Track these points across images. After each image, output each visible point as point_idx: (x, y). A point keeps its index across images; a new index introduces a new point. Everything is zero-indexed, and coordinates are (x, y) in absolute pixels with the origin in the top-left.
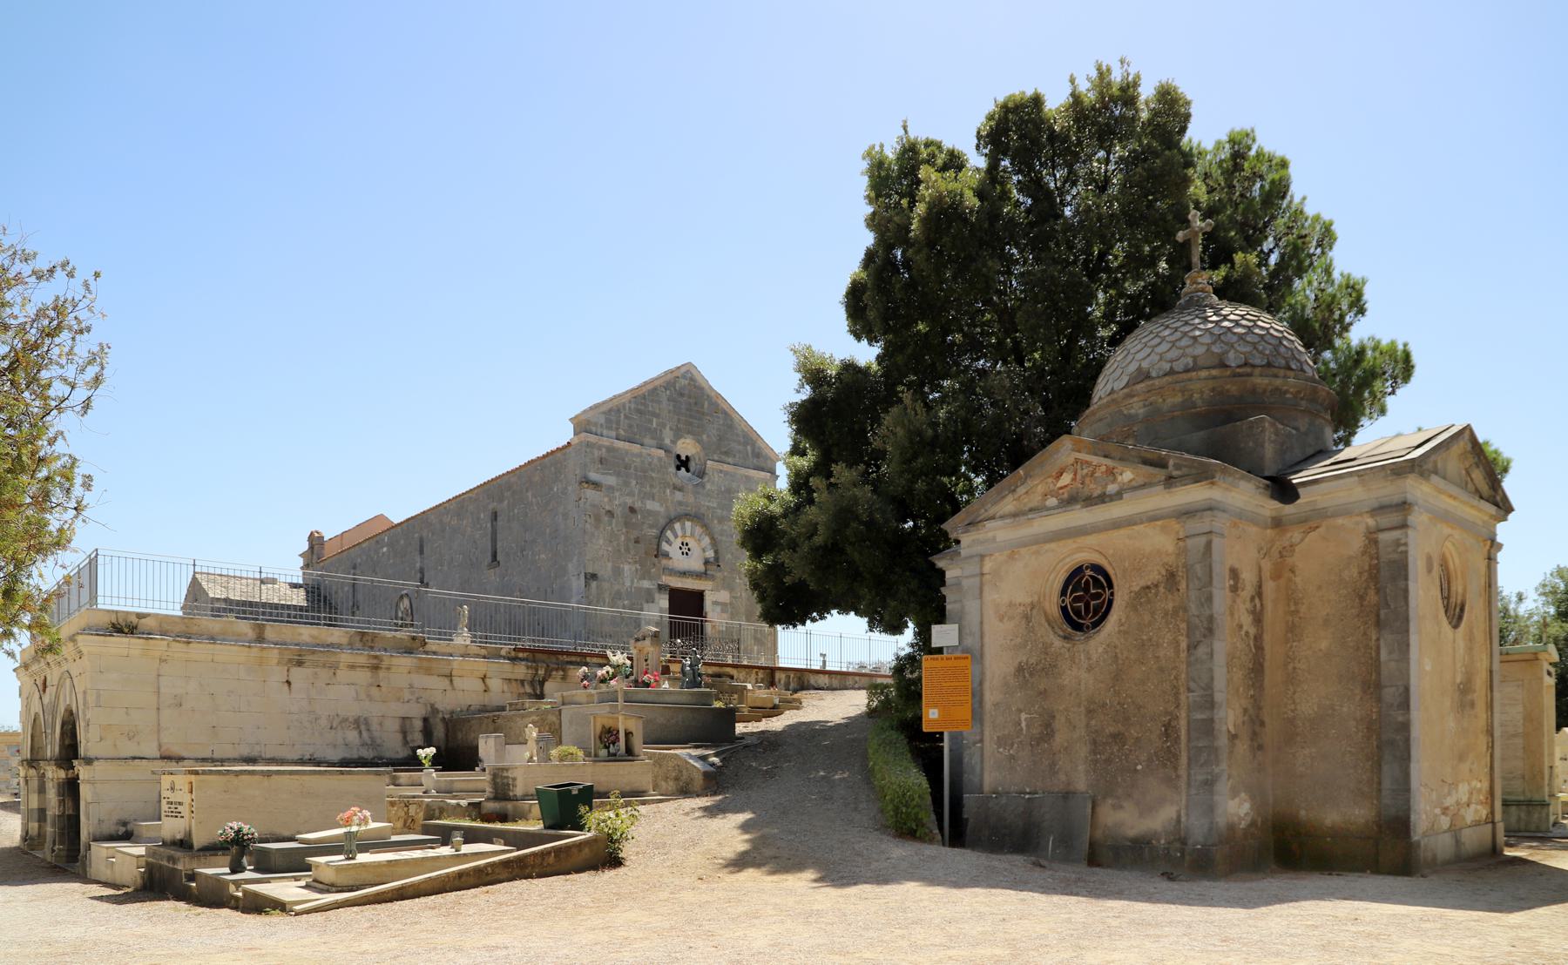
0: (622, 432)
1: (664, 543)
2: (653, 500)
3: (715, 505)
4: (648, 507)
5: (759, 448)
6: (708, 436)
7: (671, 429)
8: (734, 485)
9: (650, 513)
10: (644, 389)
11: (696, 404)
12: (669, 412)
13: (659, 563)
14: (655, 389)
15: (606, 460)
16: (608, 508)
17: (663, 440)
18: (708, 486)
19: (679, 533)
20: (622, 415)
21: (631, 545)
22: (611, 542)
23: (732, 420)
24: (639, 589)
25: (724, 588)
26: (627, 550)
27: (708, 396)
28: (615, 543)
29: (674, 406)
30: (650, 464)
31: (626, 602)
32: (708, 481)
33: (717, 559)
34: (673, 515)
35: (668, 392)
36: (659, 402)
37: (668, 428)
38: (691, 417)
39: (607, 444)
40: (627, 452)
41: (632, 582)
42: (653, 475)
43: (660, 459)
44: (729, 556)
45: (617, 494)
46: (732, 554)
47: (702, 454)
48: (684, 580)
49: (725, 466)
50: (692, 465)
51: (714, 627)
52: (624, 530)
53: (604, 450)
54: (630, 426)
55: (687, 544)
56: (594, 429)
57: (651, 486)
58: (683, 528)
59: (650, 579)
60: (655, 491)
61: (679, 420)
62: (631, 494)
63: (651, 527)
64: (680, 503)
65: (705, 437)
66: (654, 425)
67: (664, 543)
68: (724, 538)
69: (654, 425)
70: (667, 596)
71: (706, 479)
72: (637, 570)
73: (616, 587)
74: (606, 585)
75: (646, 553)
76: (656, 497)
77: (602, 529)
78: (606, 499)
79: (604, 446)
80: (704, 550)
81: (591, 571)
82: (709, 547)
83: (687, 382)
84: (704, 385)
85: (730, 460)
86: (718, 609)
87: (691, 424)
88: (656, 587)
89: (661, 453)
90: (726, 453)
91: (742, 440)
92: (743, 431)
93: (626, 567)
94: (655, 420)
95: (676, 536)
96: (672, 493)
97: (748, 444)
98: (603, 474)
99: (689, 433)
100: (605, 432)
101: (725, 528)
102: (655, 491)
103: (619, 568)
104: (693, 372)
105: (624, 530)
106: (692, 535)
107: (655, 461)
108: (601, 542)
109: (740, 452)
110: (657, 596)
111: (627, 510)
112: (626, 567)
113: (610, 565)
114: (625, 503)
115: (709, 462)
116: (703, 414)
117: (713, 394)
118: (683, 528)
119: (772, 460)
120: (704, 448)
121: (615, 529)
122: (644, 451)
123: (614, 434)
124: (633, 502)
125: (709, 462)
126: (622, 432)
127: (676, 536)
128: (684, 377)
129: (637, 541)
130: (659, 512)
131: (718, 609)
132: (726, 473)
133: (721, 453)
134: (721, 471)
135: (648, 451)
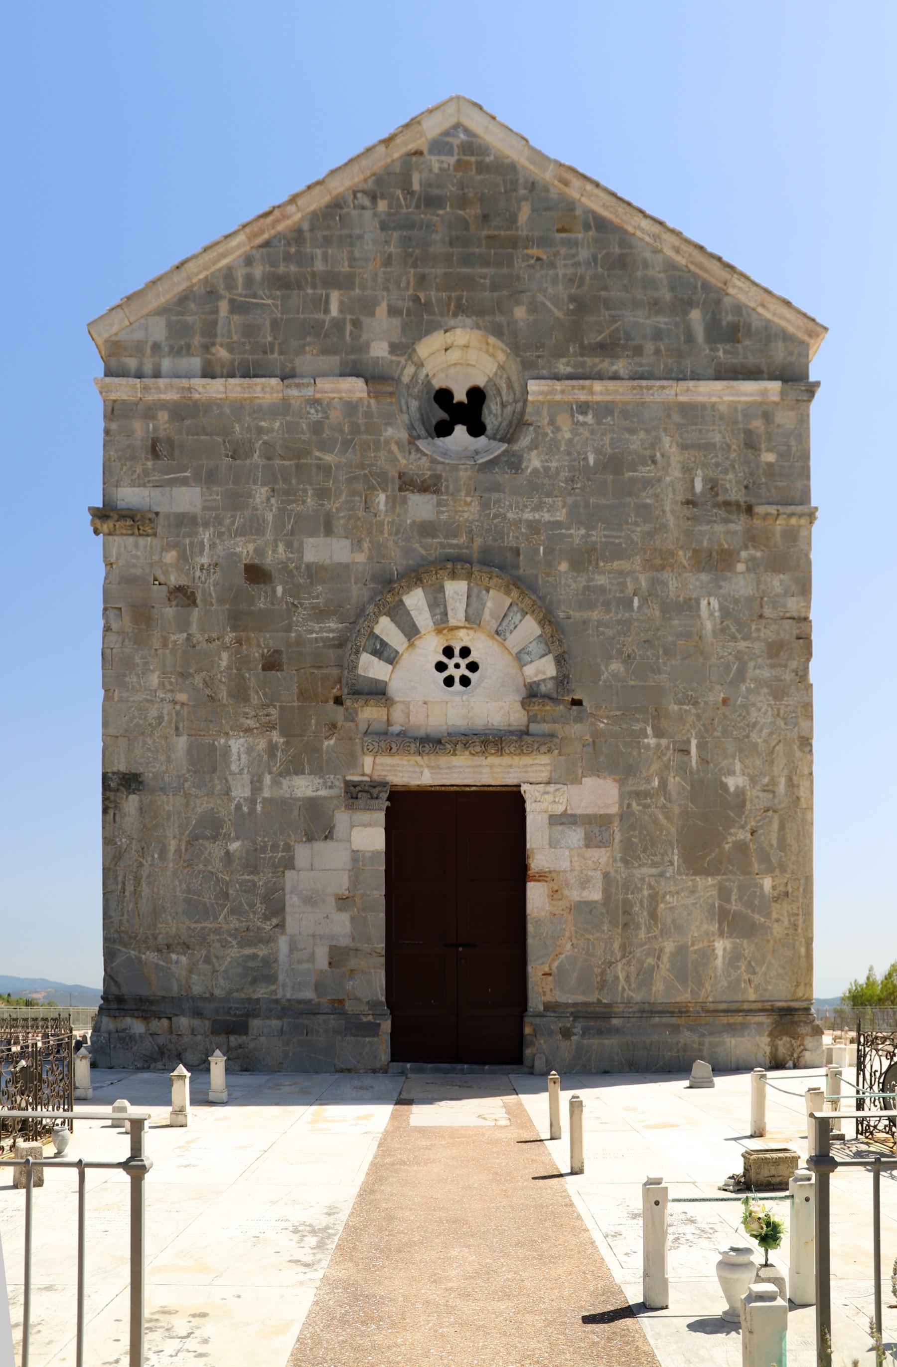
0: (222, 353)
1: (366, 658)
2: (329, 531)
3: (561, 515)
4: (310, 556)
5: (738, 309)
6: (533, 308)
7: (393, 311)
8: (636, 442)
9: (315, 573)
10: (296, 216)
11: (486, 218)
12: (388, 261)
13: (351, 717)
14: (337, 204)
15: (170, 442)
16: (174, 579)
17: (362, 348)
18: (534, 462)
19: (423, 618)
20: (224, 307)
21: (252, 679)
22: (184, 675)
23: (624, 238)
24: (282, 805)
25: (595, 770)
26: (240, 694)
27: (532, 186)
28: (198, 680)
29: (406, 242)
30: (317, 428)
31: (234, 846)
32: (534, 446)
33: (562, 681)
34: (397, 561)
35: (382, 205)
36: (349, 241)
37: (382, 310)
38: (467, 260)
39: (171, 396)
40: (238, 408)
41: (256, 785)
42: (329, 458)
43: (351, 408)
44: (616, 666)
45: (206, 536)
46: (628, 659)
47: (514, 367)
48: (443, 760)
49: (598, 386)
50: (493, 413)
51: (555, 894)
52: (230, 637)
53: (163, 416)
54: (250, 331)
55: (465, 652)
56: (132, 363)
57: (322, 494)
58: (438, 605)
59: (318, 770)
60: (333, 505)
61: (422, 280)
62: (254, 528)
63: (320, 614)
64: (426, 529)
65: (520, 313)
66: (334, 311)
67: (366, 658)
68: (595, 615)
69: (334, 311)
70: (381, 816)
71: (524, 441)
72: (272, 749)
73: (203, 805)
74: (169, 803)
75: (303, 695)
76: (339, 524)
77: (156, 644)
78: (170, 557)
79: (163, 405)
80: (520, 658)
81: (122, 768)
82: (536, 648)
83: (452, 160)
84: (513, 153)
85: (620, 366)
86: (575, 836)
87: (468, 282)
88: (339, 790)
89: (355, 388)
90: (606, 349)
91: (667, 295)
92: (671, 266)
93: (237, 745)
94: (335, 297)
95: (411, 632)
96: (392, 502)
97: (690, 304)
98: (159, 485)
99: (461, 309)
100: (166, 364)
101: (601, 580)
102: (333, 505)
103: (213, 748)
104: (476, 123)
105: (230, 637)
106: (473, 620)
107: (336, 415)
108: (154, 679)
109: (658, 335)
110: (342, 818)
111: (239, 579)
112: (237, 745)
113: (182, 743)
114: (232, 557)
115: (533, 386)
116: (514, 243)
117: (548, 175)
118: (438, 605)
119: (787, 337)
120: (515, 348)
121: (198, 637)
122: (294, 392)
123: (196, 362)
124: (260, 552)
125: (533, 386)
126: (222, 353)
127: (411, 632)
128: (439, 146)
129: (271, 664)
130: (347, 567)
131: (575, 836)
132: (605, 410)
133: (587, 350)
134: (583, 408)
135: (309, 392)
